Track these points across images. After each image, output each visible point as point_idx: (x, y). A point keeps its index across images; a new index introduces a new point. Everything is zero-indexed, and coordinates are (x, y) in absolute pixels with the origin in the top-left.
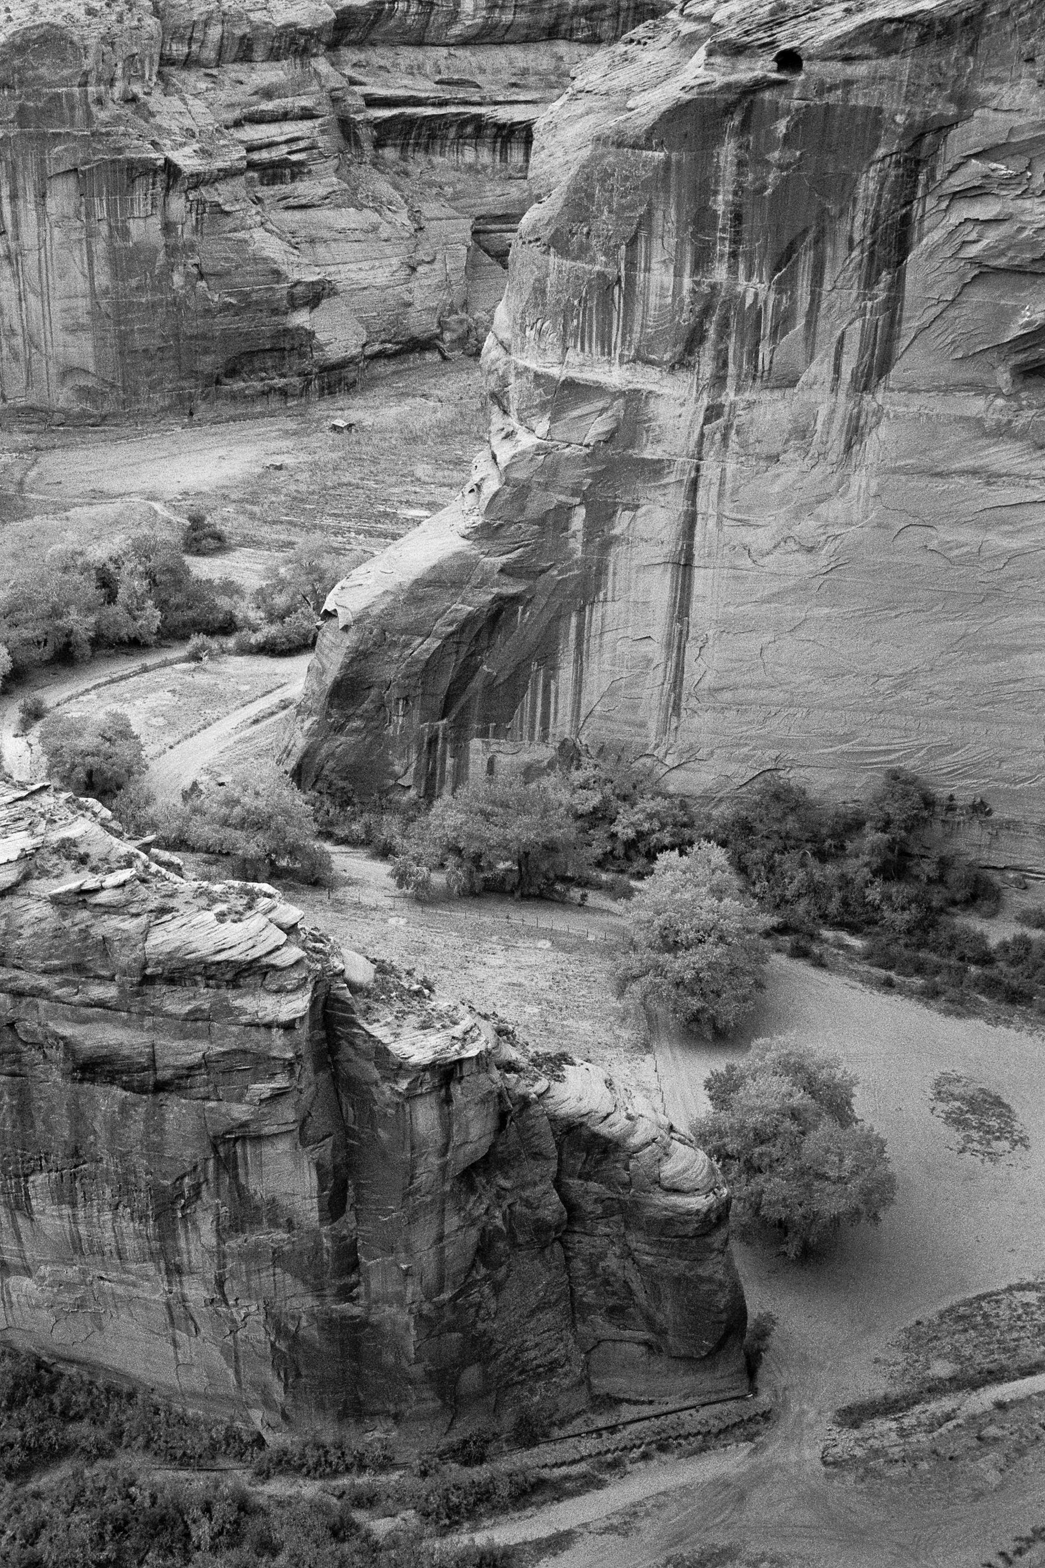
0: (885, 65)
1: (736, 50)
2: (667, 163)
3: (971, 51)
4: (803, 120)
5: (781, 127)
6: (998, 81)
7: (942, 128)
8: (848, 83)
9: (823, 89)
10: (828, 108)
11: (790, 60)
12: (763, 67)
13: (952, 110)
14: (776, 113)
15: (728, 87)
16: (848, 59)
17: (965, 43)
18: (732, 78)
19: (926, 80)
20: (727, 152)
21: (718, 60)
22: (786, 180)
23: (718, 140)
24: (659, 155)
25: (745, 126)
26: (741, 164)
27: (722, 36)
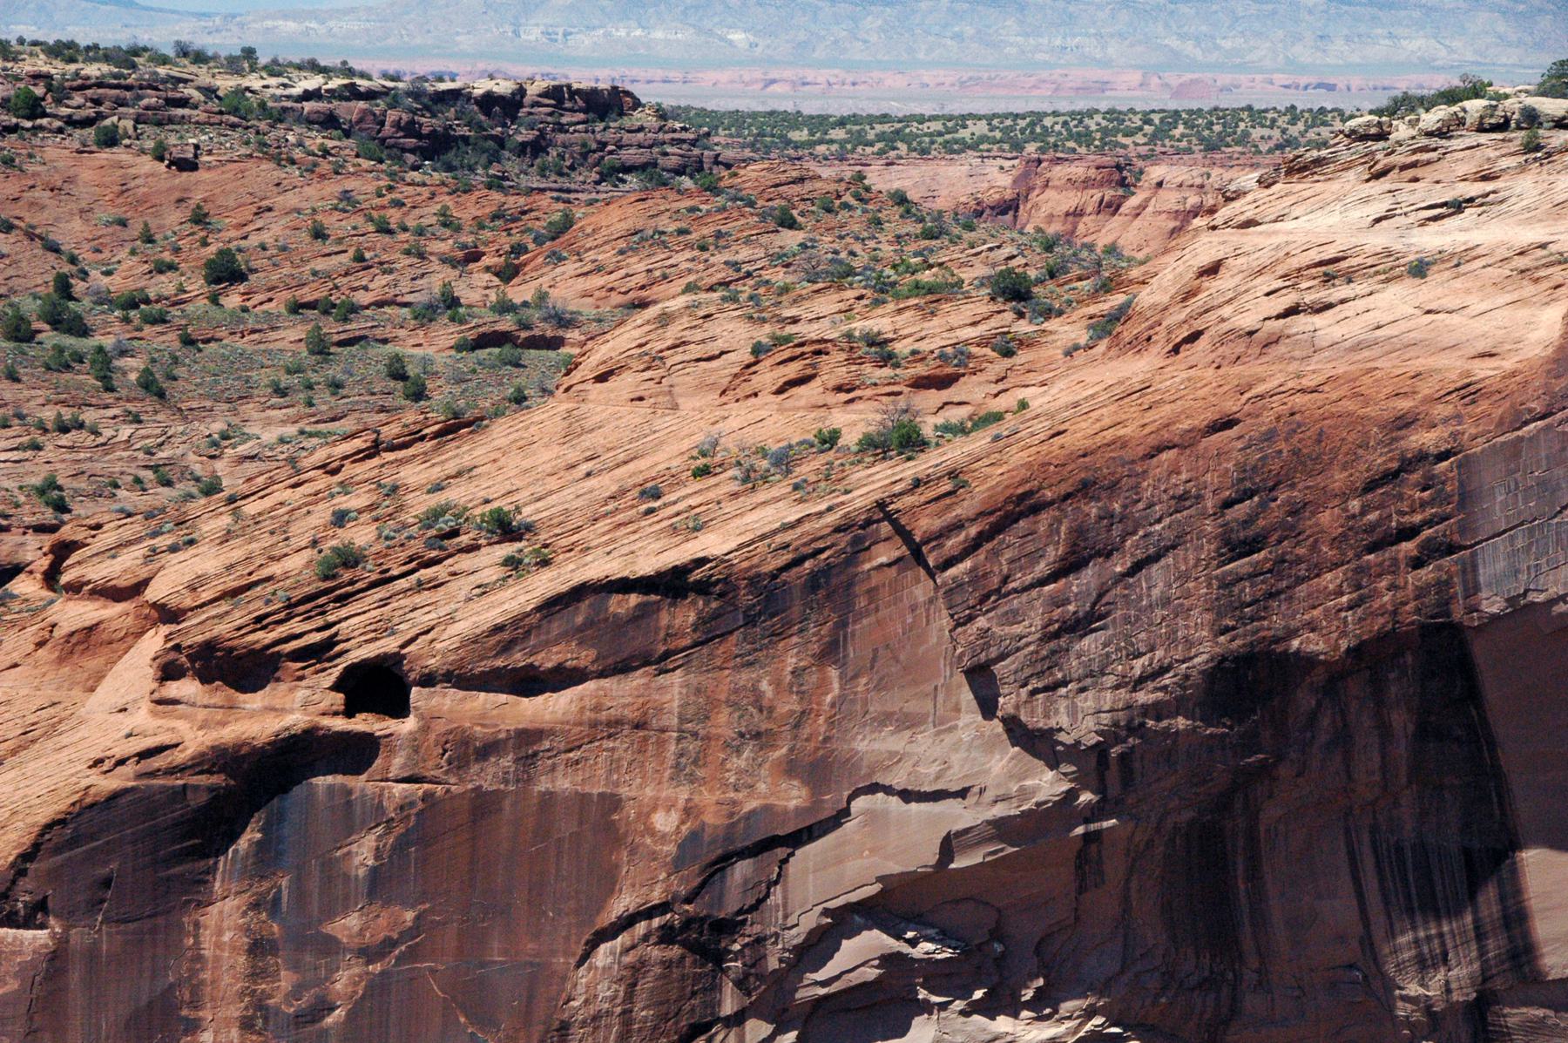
0: (621, 693)
1: (238, 669)
2: (57, 958)
3: (831, 652)
4: (421, 836)
5: (363, 852)
6: (909, 722)
7: (780, 842)
8: (528, 739)
9: (468, 750)
10: (483, 805)
11: (380, 686)
12: (296, 705)
13: (794, 796)
14: (350, 818)
15: (220, 759)
16: (529, 683)
17: (817, 632)
18: (233, 731)
19: (724, 723)
20: (223, 921)
21: (187, 688)
22: (377, 988)
23: (196, 891)
24: (35, 939)
25: (266, 858)
26: (259, 948)
27: (195, 631)
